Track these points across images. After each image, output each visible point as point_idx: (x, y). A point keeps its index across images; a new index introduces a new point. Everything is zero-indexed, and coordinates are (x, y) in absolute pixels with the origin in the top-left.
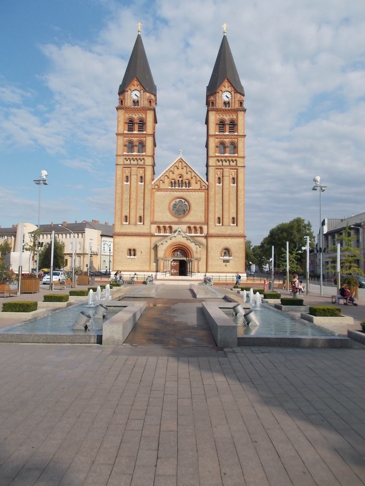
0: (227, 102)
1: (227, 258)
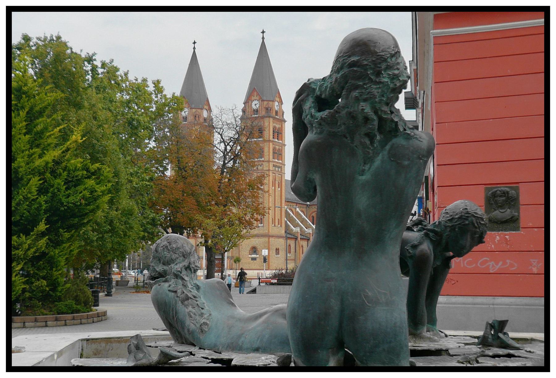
0: (256, 110)
1: (253, 256)
